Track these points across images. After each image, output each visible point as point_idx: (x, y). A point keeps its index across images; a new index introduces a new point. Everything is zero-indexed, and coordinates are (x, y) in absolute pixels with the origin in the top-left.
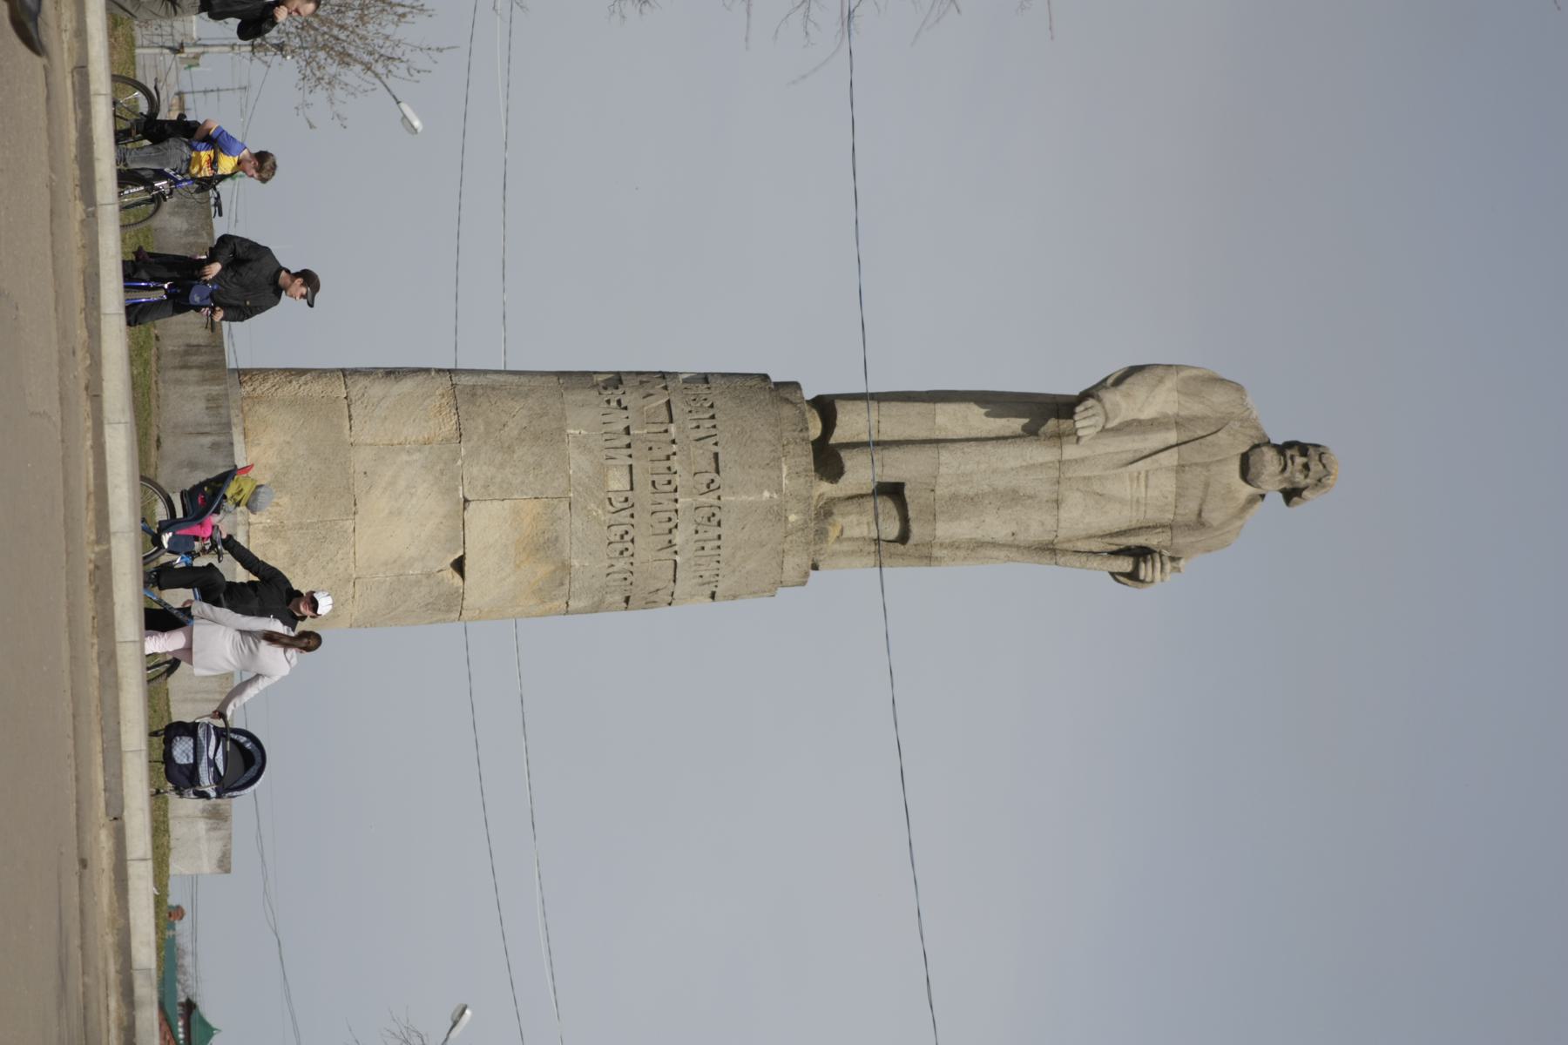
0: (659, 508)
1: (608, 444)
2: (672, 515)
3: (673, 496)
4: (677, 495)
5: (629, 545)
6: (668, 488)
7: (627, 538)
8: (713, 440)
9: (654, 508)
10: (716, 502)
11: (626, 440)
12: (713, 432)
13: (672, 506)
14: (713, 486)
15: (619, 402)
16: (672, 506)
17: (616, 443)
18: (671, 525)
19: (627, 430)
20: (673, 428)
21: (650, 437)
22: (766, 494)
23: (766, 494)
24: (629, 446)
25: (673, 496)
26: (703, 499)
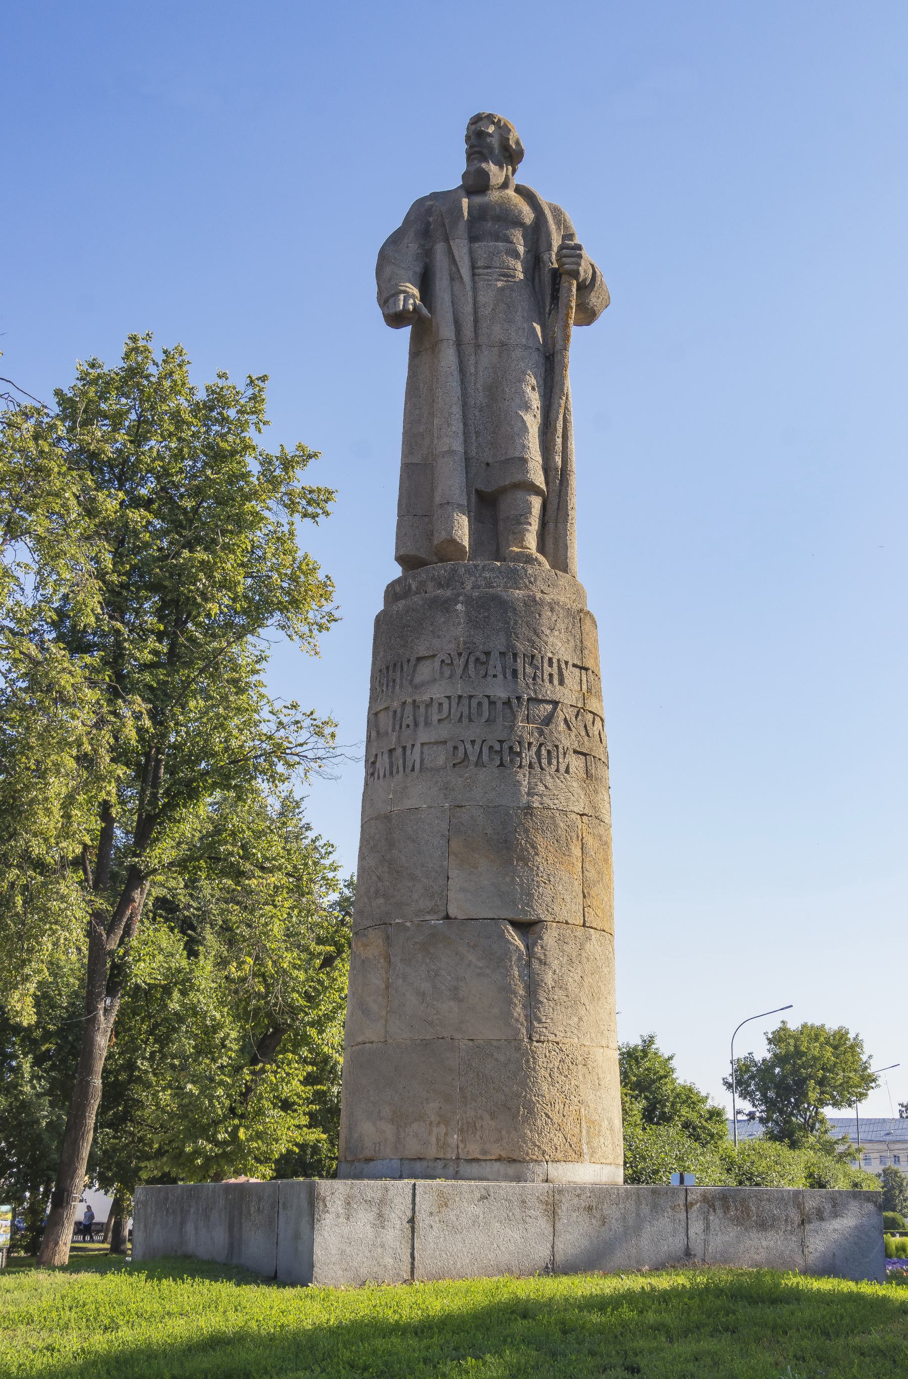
0: (466, 713)
1: (401, 769)
2: (474, 703)
5: (506, 746)
6: (446, 706)
7: (497, 747)
9: (465, 720)
11: (399, 751)
12: (399, 664)
13: (465, 702)
16: (465, 702)
17: (401, 762)
18: (486, 702)
19: (391, 751)
21: (397, 727)
23: (459, 607)
24: (404, 748)
25: (454, 703)
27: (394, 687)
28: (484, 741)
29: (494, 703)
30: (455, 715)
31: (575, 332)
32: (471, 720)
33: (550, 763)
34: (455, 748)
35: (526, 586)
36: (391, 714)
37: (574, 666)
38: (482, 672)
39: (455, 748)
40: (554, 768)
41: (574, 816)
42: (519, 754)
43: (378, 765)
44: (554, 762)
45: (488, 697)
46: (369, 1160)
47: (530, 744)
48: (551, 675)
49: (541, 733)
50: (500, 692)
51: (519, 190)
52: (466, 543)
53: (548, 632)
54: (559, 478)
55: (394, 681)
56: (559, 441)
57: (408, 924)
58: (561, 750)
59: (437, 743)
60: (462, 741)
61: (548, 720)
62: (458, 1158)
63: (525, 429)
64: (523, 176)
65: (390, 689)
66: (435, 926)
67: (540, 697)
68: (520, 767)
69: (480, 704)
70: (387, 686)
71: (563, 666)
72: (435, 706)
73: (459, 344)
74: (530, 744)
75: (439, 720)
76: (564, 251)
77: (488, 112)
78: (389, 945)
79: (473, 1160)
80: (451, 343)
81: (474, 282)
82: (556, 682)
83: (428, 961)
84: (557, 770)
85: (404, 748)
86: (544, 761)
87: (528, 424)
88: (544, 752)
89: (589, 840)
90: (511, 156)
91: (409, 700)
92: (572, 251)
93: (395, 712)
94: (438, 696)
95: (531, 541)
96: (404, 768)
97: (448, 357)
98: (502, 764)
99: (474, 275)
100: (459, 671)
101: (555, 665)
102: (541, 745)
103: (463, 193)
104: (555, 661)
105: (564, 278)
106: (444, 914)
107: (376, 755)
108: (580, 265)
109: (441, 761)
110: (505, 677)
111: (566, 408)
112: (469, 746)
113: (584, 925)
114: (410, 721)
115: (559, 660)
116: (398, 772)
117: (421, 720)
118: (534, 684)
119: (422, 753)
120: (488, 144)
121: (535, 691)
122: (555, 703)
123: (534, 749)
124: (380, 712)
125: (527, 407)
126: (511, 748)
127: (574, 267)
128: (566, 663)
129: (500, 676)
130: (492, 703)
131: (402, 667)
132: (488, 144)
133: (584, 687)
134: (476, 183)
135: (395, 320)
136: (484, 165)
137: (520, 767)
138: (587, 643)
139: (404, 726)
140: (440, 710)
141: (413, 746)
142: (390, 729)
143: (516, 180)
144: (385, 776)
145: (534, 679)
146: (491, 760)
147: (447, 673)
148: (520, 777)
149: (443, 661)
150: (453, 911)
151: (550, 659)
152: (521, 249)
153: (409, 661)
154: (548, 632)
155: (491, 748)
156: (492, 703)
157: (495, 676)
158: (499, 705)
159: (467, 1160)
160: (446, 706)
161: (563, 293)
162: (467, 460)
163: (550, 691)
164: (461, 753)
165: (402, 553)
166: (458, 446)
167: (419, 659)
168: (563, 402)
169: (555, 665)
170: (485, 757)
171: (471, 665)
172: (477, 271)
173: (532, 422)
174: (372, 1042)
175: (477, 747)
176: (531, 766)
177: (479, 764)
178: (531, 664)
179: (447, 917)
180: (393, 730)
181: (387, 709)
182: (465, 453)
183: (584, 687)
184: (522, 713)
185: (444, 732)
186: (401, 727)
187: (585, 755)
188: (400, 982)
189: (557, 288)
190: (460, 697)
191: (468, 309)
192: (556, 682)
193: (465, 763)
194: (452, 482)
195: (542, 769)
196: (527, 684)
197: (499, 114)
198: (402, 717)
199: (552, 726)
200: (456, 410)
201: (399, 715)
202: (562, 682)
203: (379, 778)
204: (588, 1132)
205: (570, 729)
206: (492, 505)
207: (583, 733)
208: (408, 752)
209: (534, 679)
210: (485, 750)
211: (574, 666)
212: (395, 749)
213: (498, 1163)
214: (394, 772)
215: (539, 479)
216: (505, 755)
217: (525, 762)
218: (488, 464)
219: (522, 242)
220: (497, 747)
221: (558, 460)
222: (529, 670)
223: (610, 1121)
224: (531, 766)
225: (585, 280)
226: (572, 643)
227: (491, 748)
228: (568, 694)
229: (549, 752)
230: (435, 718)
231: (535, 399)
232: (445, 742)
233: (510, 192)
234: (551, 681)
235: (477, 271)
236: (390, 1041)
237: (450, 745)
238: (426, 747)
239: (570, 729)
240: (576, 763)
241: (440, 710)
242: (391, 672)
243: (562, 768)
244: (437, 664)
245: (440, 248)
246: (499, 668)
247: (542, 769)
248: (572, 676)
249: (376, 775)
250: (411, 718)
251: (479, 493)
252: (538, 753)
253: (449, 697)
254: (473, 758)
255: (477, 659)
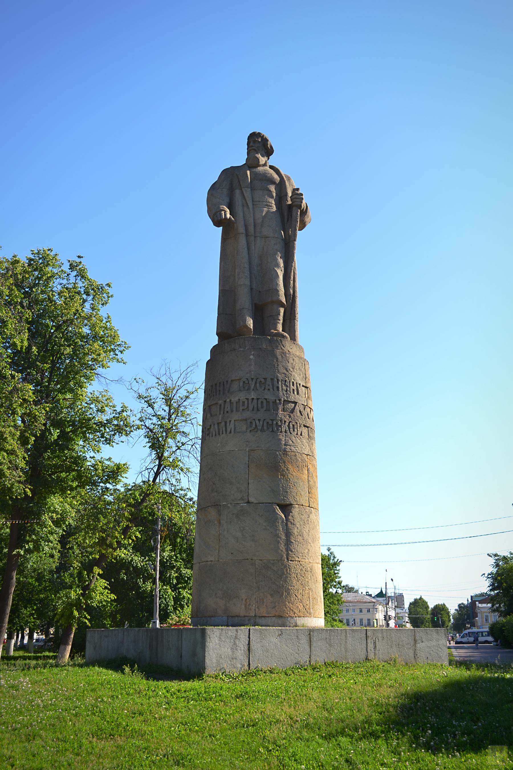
0: (256, 406)
1: (224, 432)
2: (260, 401)
3: (250, 401)
4: (250, 398)
6: (246, 403)
7: (270, 422)
8: (225, 383)
10: (254, 380)
11: (223, 424)
12: (222, 383)
13: (255, 401)
14: (247, 382)
15: (208, 429)
17: (224, 429)
18: (265, 401)
19: (218, 424)
20: (220, 402)
21: (222, 412)
22: (252, 357)
24: (226, 423)
25: (250, 401)
26: (252, 387)
27: (219, 394)
28: (264, 420)
29: (269, 402)
30: (251, 407)
31: (298, 233)
32: (258, 410)
33: (294, 431)
34: (251, 423)
35: (281, 348)
36: (218, 406)
37: (303, 386)
38: (263, 388)
39: (251, 423)
40: (296, 433)
41: (304, 455)
42: (280, 426)
43: (211, 430)
44: (296, 430)
45: (266, 399)
46: (211, 617)
47: (285, 421)
48: (293, 390)
49: (290, 417)
50: (271, 397)
51: (271, 167)
52: (252, 328)
53: (292, 370)
54: (292, 299)
55: (220, 391)
56: (292, 282)
57: (229, 505)
58: (298, 425)
59: (242, 420)
60: (254, 420)
61: (293, 411)
62: (255, 616)
63: (278, 276)
64: (273, 161)
65: (218, 394)
66: (242, 506)
67: (289, 400)
68: (281, 432)
69: (262, 402)
70: (216, 393)
71: (298, 386)
72: (241, 403)
73: (247, 235)
74: (285, 421)
75: (243, 410)
76: (295, 196)
77: (258, 131)
78: (220, 515)
79: (262, 617)
80: (244, 235)
81: (253, 208)
82: (296, 393)
83: (239, 522)
84: (297, 434)
85: (226, 423)
86: (291, 430)
87: (279, 274)
88: (291, 426)
89: (310, 466)
90: (269, 152)
91: (228, 400)
92: (297, 196)
93: (221, 405)
94: (242, 398)
95: (280, 328)
96: (226, 431)
97: (242, 241)
98: (273, 431)
99: (253, 204)
100: (252, 387)
101: (295, 385)
102: (290, 422)
103: (246, 167)
104: (295, 383)
105: (294, 208)
106: (247, 501)
107: (211, 425)
108: (302, 202)
109: (244, 428)
110: (273, 390)
111: (295, 268)
112: (257, 422)
113: (309, 506)
114: (229, 409)
115: (297, 383)
116: (223, 433)
117: (234, 409)
118: (286, 394)
119: (235, 425)
120: (259, 144)
121: (287, 397)
122: (295, 403)
123: (287, 424)
124: (212, 405)
125: (278, 266)
126: (277, 423)
127: (299, 203)
128: (300, 384)
129: (271, 390)
130: (268, 402)
131: (224, 384)
132: (259, 144)
133: (307, 396)
134: (252, 163)
135: (217, 222)
136: (257, 155)
137: (281, 432)
138: (307, 376)
139: (225, 412)
140: (243, 405)
141: (230, 421)
142: (218, 413)
143: (271, 162)
144: (216, 435)
145: (286, 391)
146: (268, 428)
147: (246, 388)
148: (281, 437)
149: (244, 382)
150: (252, 499)
151: (293, 382)
152: (274, 194)
153: (227, 381)
154: (292, 370)
155: (268, 423)
156: (268, 402)
157: (269, 390)
158: (271, 404)
159: (260, 617)
160: (246, 403)
161: (294, 214)
162: (251, 289)
163: (293, 397)
164: (254, 426)
165: (220, 331)
166: (248, 282)
167: (232, 381)
168: (293, 265)
169: (295, 385)
170: (265, 428)
171: (258, 385)
172: (254, 203)
173: (281, 274)
174: (211, 561)
175: (261, 423)
176: (286, 432)
177: (262, 430)
178: (285, 384)
179: (248, 502)
180: (220, 414)
181: (217, 403)
182: (251, 286)
183: (307, 396)
184: (281, 407)
185: (247, 414)
186: (224, 413)
187: (308, 427)
188: (226, 533)
189: (291, 213)
190: (253, 399)
191: (251, 220)
192: (296, 393)
193: (256, 430)
194: (244, 300)
195: (291, 433)
196: (283, 394)
197: (263, 132)
198: (224, 408)
199: (294, 414)
200: (247, 266)
201: (223, 406)
202: (298, 393)
203: (212, 436)
204: (313, 603)
205: (302, 415)
206: (263, 311)
207: (307, 417)
208: (228, 424)
209: (286, 391)
210: (265, 424)
211: (303, 386)
212: (221, 423)
213: (274, 618)
214: (221, 433)
215: (283, 300)
216: (273, 427)
217: (283, 430)
218: (260, 292)
219: (274, 191)
220: (270, 422)
221: (292, 291)
222: (284, 388)
223: (320, 597)
224: (286, 432)
225: (303, 209)
226: (302, 376)
227: (268, 423)
228: (301, 400)
229: (293, 425)
230: (241, 408)
231: (281, 262)
232: (246, 420)
233: (267, 168)
234: (294, 393)
235: (254, 203)
236: (221, 560)
237: (249, 421)
238: (236, 422)
239: (302, 415)
240: (305, 431)
241: (243, 405)
242: (218, 388)
243: (299, 434)
244: (241, 384)
245: (237, 192)
246: (271, 386)
247: (291, 433)
248: (302, 390)
249: (211, 435)
250: (229, 408)
251: (255, 304)
252: (289, 426)
253: (247, 399)
254: (260, 428)
255: (261, 381)
